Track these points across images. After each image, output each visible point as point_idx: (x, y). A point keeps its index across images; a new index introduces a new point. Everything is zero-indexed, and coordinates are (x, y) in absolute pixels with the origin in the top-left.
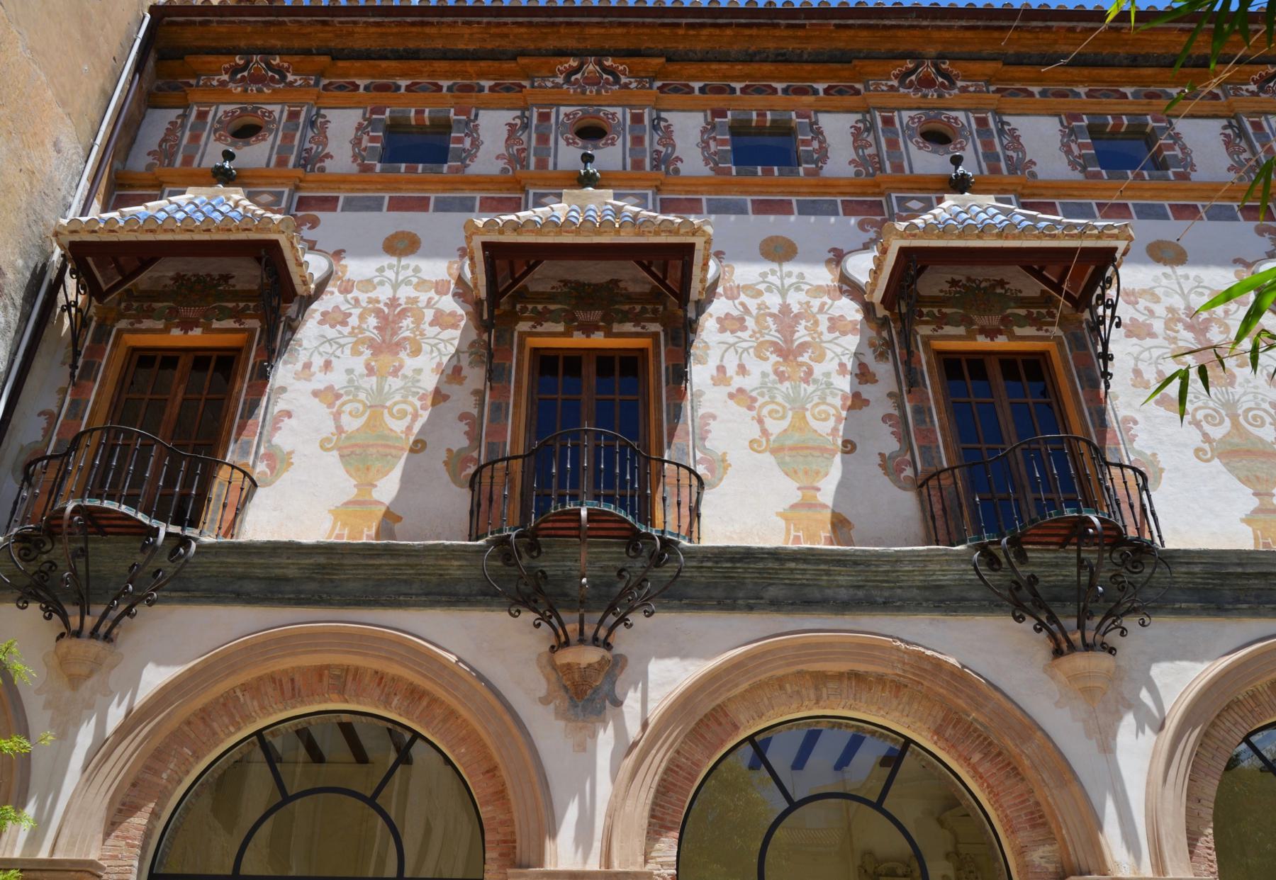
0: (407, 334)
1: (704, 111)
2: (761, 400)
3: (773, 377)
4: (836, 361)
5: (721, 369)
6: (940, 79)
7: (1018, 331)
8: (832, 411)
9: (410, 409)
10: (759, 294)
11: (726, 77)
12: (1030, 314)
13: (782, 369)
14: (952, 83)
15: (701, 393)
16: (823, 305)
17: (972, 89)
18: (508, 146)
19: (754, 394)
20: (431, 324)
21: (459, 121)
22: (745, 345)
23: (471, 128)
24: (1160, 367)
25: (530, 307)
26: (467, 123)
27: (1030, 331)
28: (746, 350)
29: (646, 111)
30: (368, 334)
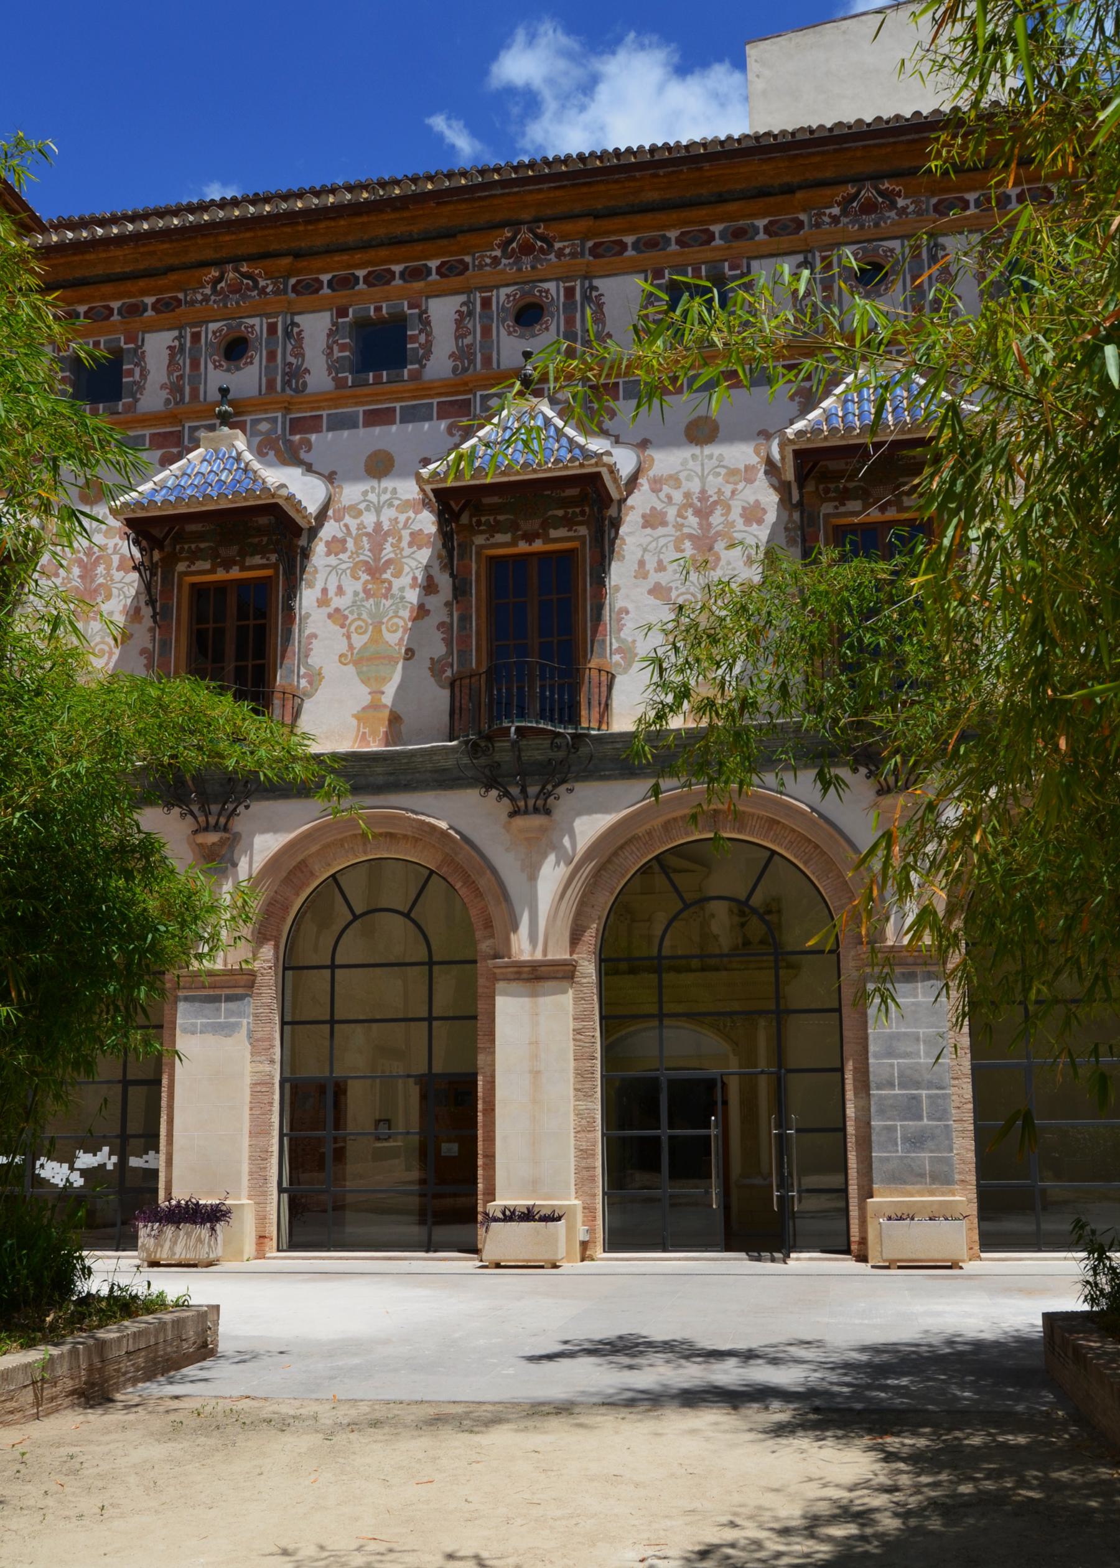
0: (101, 580)
1: (331, 309)
2: (351, 618)
3: (362, 595)
4: (411, 575)
5: (325, 591)
6: (539, 243)
7: (553, 533)
8: (401, 623)
9: (107, 648)
10: (360, 513)
11: (350, 267)
12: (567, 513)
13: (370, 586)
14: (550, 246)
15: (308, 615)
16: (408, 519)
17: (567, 251)
18: (170, 373)
19: (346, 613)
20: (118, 570)
21: (128, 349)
22: (344, 566)
23: (138, 356)
24: (662, 556)
25: (186, 547)
26: (135, 350)
27: (561, 532)
28: (344, 571)
29: (280, 319)
30: (74, 583)
